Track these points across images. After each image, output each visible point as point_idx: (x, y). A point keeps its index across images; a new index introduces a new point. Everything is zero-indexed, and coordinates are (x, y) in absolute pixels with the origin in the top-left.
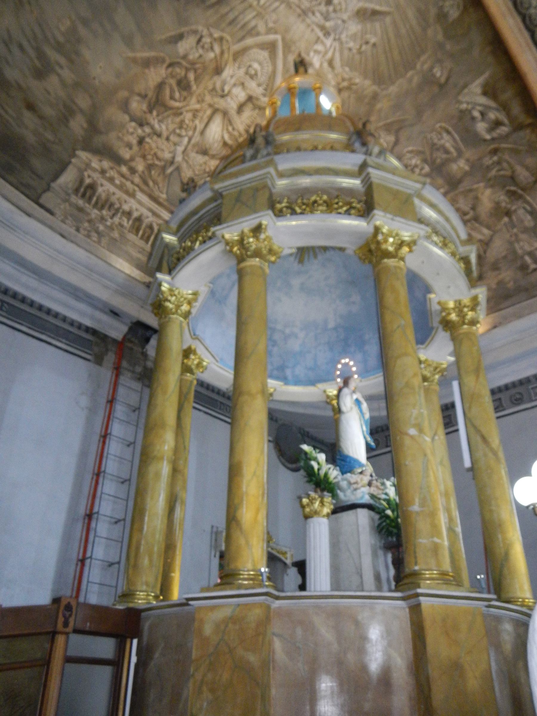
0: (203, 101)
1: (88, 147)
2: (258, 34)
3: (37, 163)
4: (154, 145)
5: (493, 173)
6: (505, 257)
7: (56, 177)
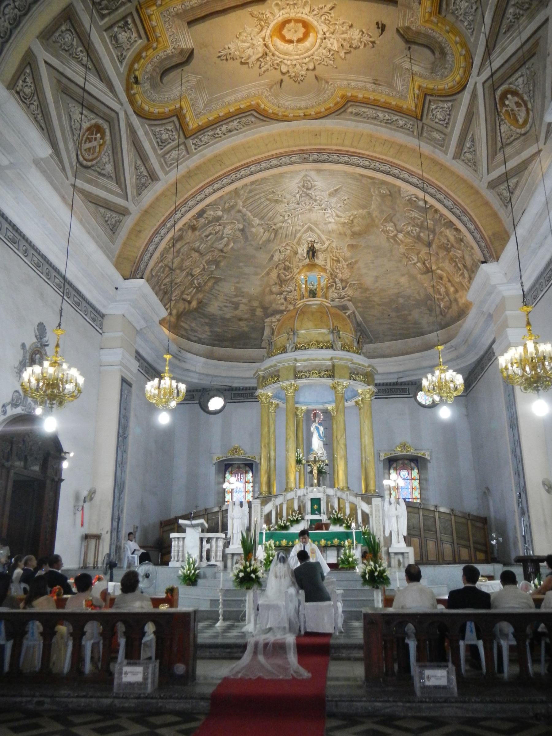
2: (300, 230)
3: (254, 335)
4: (291, 297)
5: (443, 222)
6: (473, 264)
7: (263, 334)
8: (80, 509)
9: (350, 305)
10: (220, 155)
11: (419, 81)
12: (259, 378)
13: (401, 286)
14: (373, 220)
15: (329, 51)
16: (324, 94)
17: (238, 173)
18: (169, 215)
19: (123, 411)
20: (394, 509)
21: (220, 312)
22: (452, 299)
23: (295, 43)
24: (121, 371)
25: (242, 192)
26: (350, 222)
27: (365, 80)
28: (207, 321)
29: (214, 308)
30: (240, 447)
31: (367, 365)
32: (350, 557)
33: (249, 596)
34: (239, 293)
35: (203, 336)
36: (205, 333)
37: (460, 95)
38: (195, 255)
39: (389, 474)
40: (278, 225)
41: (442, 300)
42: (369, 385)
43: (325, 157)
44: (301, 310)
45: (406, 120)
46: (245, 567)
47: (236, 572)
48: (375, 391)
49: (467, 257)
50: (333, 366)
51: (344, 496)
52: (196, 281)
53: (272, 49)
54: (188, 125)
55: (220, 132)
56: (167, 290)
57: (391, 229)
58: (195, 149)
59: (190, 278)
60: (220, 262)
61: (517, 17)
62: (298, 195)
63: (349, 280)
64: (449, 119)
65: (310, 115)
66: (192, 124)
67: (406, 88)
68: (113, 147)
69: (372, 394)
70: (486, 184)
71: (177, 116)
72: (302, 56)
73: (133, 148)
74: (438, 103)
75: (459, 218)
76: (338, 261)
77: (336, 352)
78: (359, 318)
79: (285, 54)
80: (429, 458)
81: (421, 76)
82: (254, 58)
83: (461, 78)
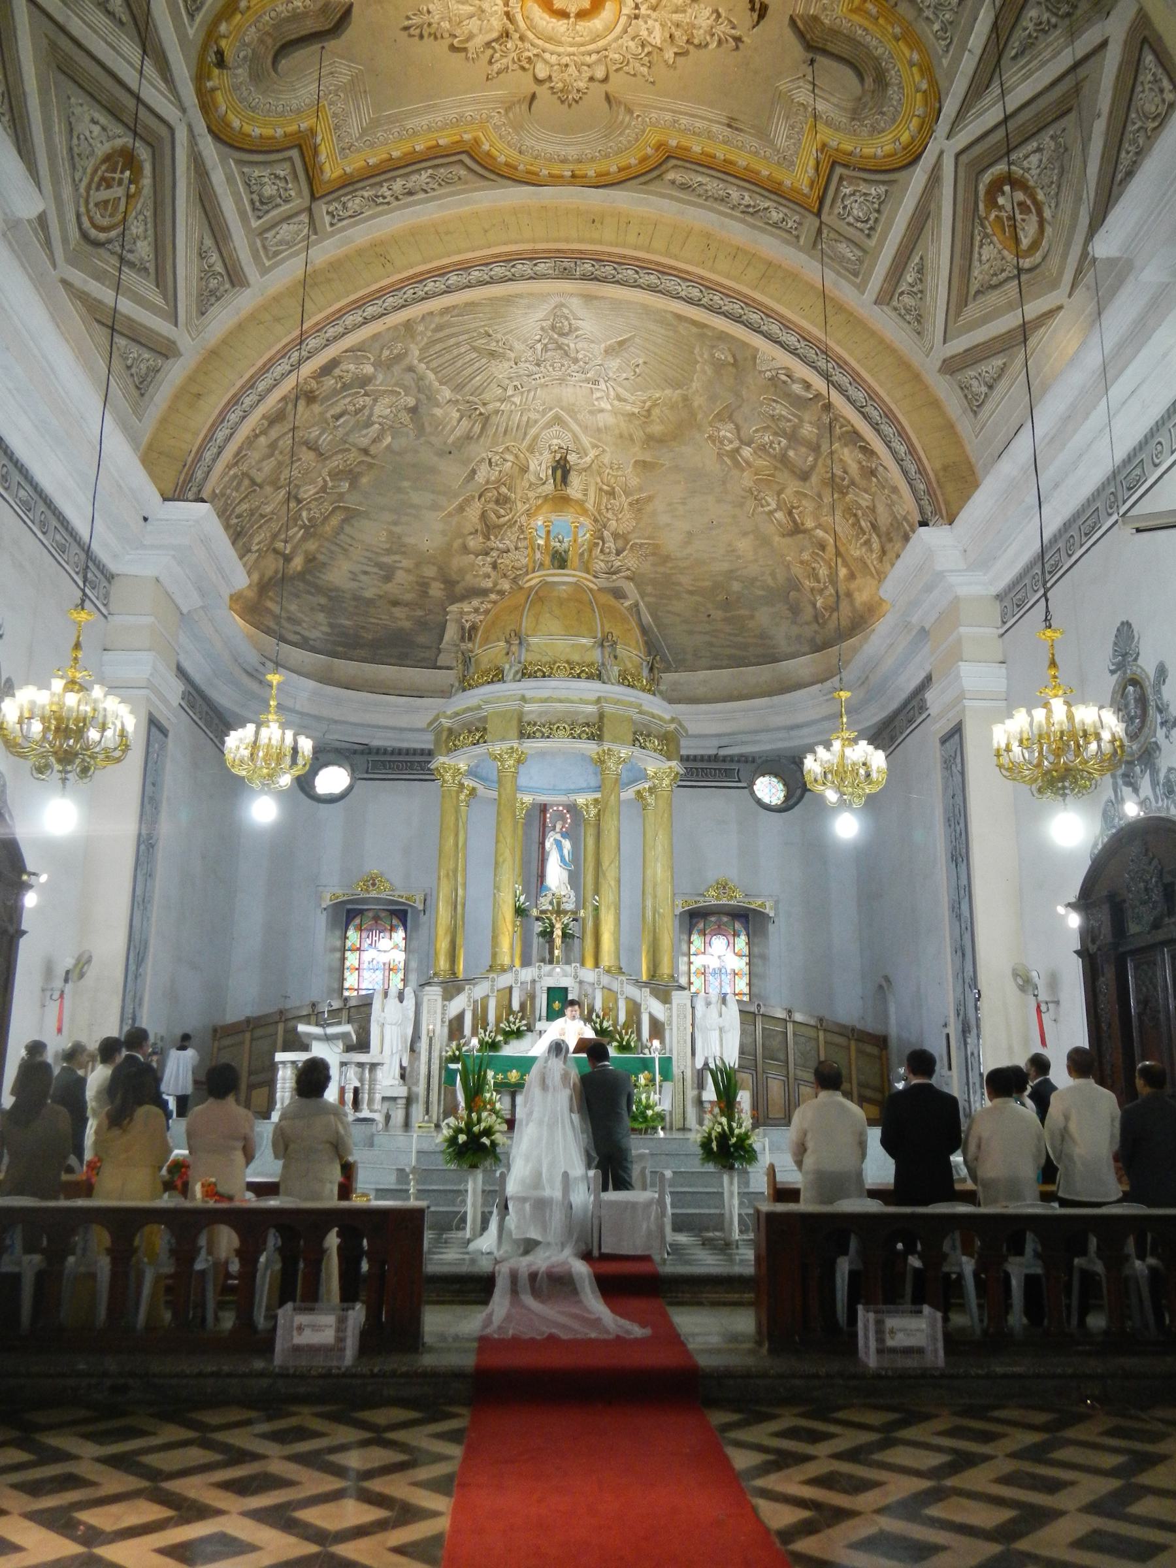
0: (528, 500)
1: (454, 599)
2: (536, 422)
3: (421, 639)
4: (508, 562)
8: (56, 995)
9: (630, 588)
10: (382, 243)
11: (826, 134)
12: (441, 732)
13: (739, 557)
14: (693, 414)
15: (643, 46)
16: (621, 134)
17: (421, 286)
18: (265, 365)
19: (149, 788)
20: (715, 1014)
21: (354, 585)
22: (841, 592)
23: (572, 20)
24: (148, 699)
25: (421, 328)
26: (644, 413)
27: (710, 116)
28: (323, 601)
29: (338, 575)
30: (382, 875)
31: (667, 717)
32: (648, 1107)
33: (474, 1184)
34: (397, 546)
35: (314, 634)
36: (317, 627)
37: (904, 173)
38: (307, 456)
39: (690, 942)
40: (491, 407)
41: (821, 591)
42: (669, 759)
43: (609, 270)
44: (536, 592)
45: (785, 210)
46: (469, 1124)
47: (446, 1132)
48: (682, 772)
49: (881, 509)
50: (601, 716)
51: (615, 986)
52: (304, 514)
53: (522, 24)
54: (322, 172)
55: (389, 193)
56: (243, 528)
57: (728, 434)
58: (332, 225)
59: (292, 504)
60: (360, 474)
61: (1043, 29)
62: (539, 346)
63: (631, 536)
64: (876, 220)
65: (585, 176)
66: (331, 170)
67: (795, 144)
68: (155, 203)
69: (675, 778)
70: (939, 364)
71: (300, 147)
72: (582, 49)
73: (198, 211)
74: (858, 185)
75: (876, 427)
76: (612, 494)
77: (608, 687)
78: (647, 618)
79: (549, 39)
80: (772, 914)
81: (829, 123)
82: (480, 40)
83: (913, 138)
